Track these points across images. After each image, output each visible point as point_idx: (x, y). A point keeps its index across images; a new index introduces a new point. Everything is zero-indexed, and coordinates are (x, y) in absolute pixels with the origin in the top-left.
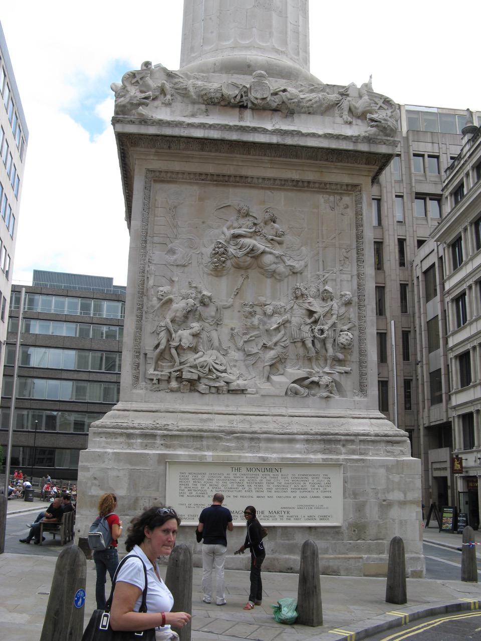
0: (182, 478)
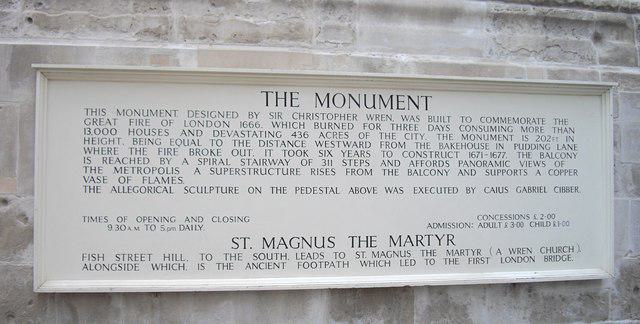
0: (93, 128)
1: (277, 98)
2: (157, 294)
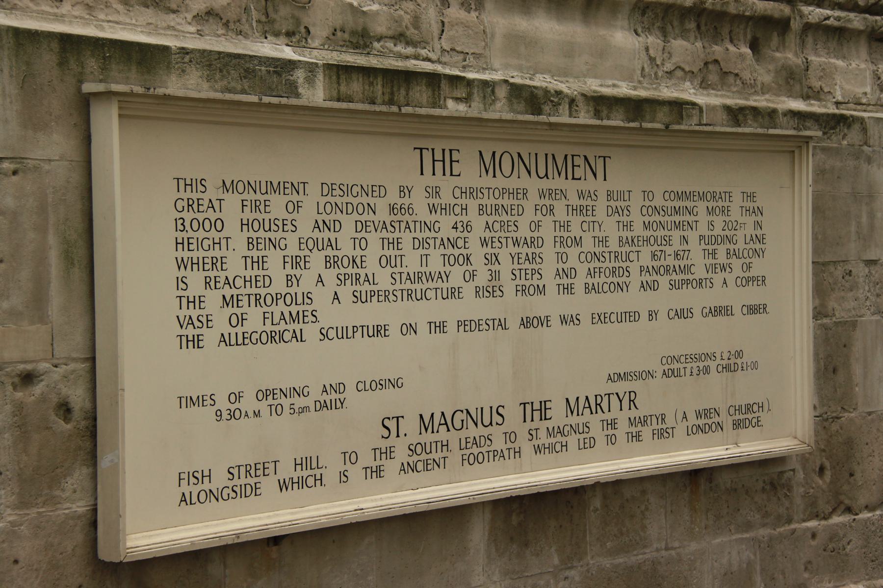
0: (188, 216)
1: (434, 161)
2: (276, 540)
